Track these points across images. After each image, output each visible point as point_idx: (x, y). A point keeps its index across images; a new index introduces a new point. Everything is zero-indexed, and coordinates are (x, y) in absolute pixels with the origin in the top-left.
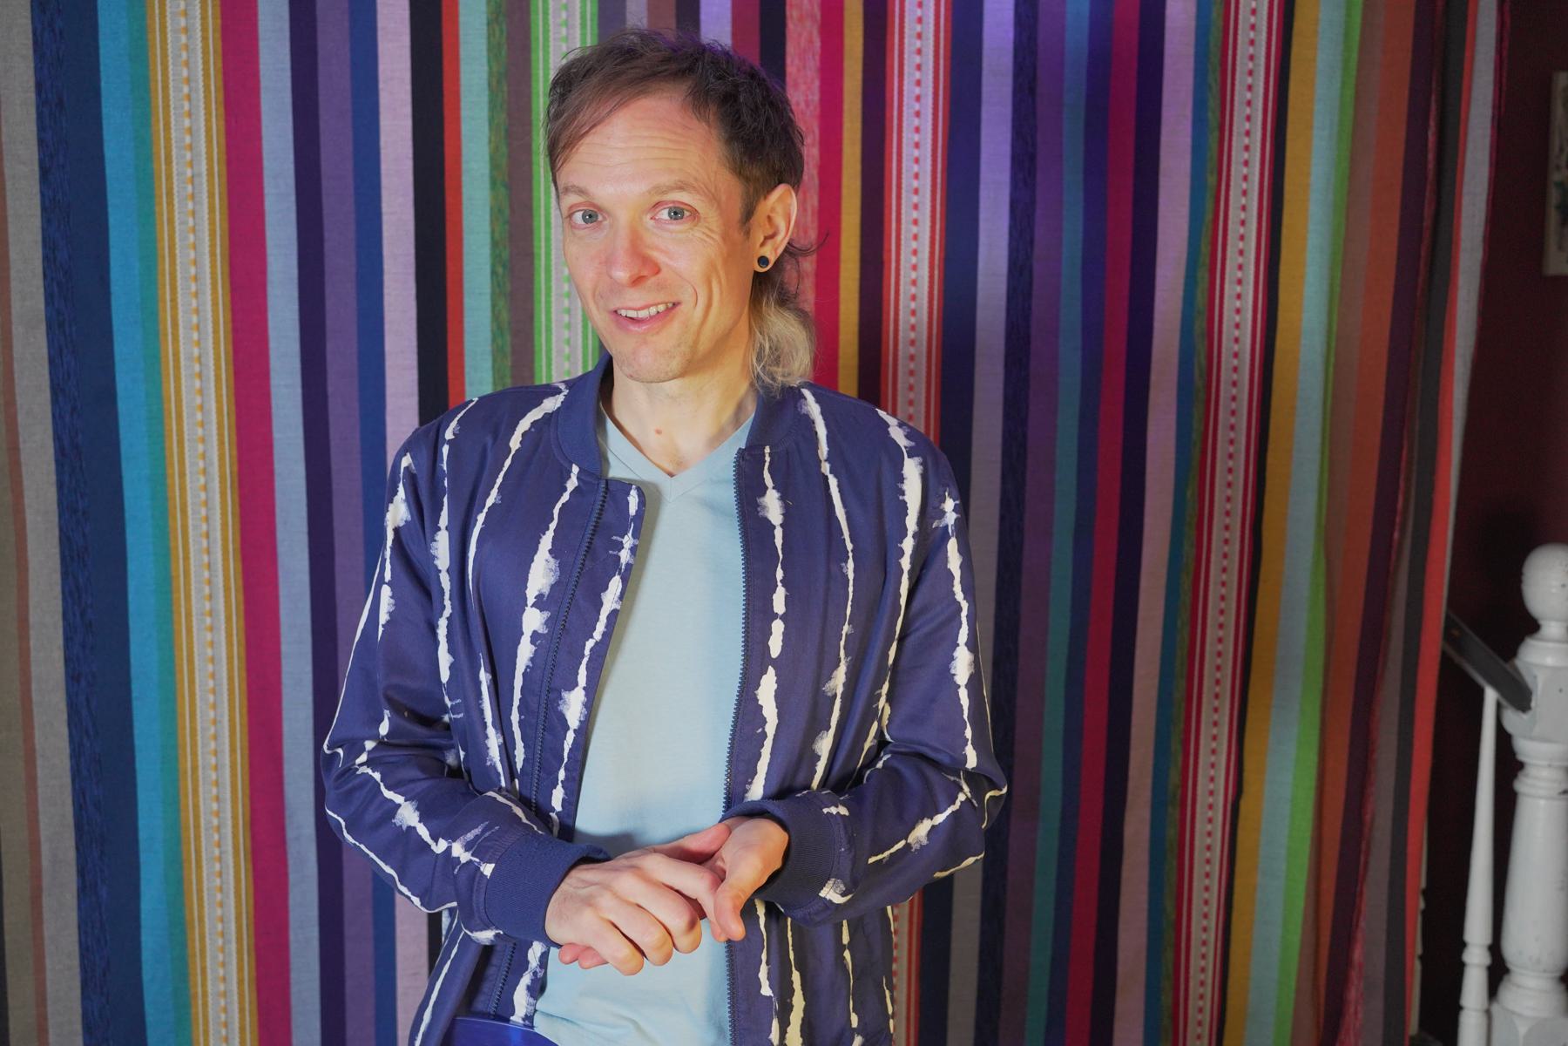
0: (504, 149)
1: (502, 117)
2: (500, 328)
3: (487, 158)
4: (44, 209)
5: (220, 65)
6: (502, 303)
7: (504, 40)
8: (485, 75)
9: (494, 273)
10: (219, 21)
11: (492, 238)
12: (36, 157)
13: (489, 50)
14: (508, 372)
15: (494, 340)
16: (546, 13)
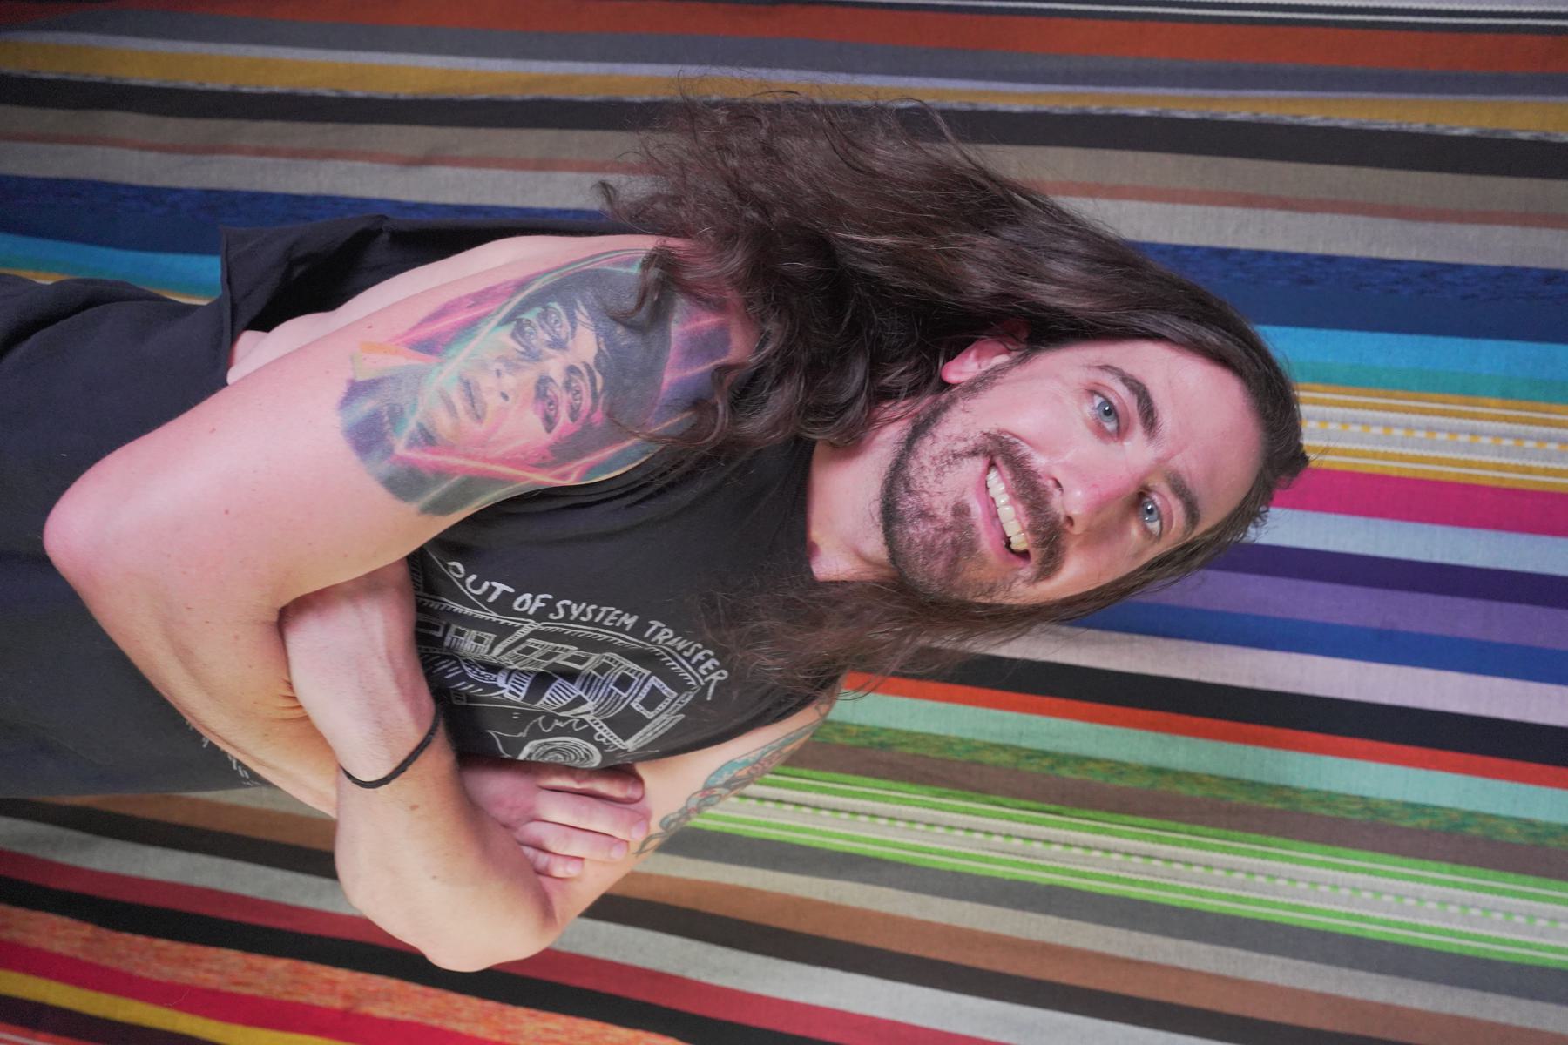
0: (1199, 792)
1: (1240, 798)
2: (977, 749)
3: (1191, 769)
4: (1178, 248)
5: (1339, 468)
6: (1004, 758)
7: (1341, 814)
8: (1296, 784)
9: (1044, 754)
10: (1395, 473)
11: (1089, 759)
12: (1243, 246)
13: (1329, 794)
14: (921, 751)
15: (962, 741)
16: (1371, 872)
